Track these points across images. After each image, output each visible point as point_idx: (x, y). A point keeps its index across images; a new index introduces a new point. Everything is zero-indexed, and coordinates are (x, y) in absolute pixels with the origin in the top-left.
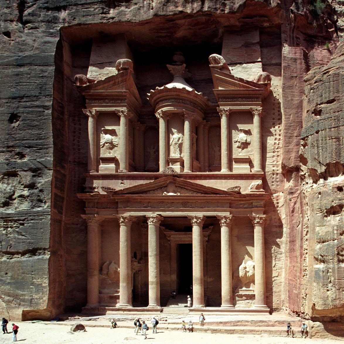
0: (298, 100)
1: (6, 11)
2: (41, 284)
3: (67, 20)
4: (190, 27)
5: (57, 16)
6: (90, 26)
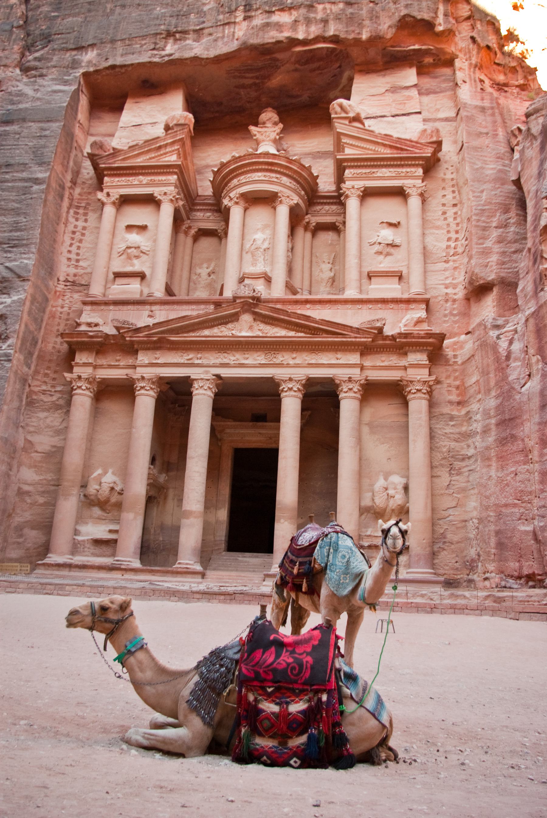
0: (495, 168)
3: (94, 62)
4: (297, 66)
5: (79, 59)
6: (130, 68)
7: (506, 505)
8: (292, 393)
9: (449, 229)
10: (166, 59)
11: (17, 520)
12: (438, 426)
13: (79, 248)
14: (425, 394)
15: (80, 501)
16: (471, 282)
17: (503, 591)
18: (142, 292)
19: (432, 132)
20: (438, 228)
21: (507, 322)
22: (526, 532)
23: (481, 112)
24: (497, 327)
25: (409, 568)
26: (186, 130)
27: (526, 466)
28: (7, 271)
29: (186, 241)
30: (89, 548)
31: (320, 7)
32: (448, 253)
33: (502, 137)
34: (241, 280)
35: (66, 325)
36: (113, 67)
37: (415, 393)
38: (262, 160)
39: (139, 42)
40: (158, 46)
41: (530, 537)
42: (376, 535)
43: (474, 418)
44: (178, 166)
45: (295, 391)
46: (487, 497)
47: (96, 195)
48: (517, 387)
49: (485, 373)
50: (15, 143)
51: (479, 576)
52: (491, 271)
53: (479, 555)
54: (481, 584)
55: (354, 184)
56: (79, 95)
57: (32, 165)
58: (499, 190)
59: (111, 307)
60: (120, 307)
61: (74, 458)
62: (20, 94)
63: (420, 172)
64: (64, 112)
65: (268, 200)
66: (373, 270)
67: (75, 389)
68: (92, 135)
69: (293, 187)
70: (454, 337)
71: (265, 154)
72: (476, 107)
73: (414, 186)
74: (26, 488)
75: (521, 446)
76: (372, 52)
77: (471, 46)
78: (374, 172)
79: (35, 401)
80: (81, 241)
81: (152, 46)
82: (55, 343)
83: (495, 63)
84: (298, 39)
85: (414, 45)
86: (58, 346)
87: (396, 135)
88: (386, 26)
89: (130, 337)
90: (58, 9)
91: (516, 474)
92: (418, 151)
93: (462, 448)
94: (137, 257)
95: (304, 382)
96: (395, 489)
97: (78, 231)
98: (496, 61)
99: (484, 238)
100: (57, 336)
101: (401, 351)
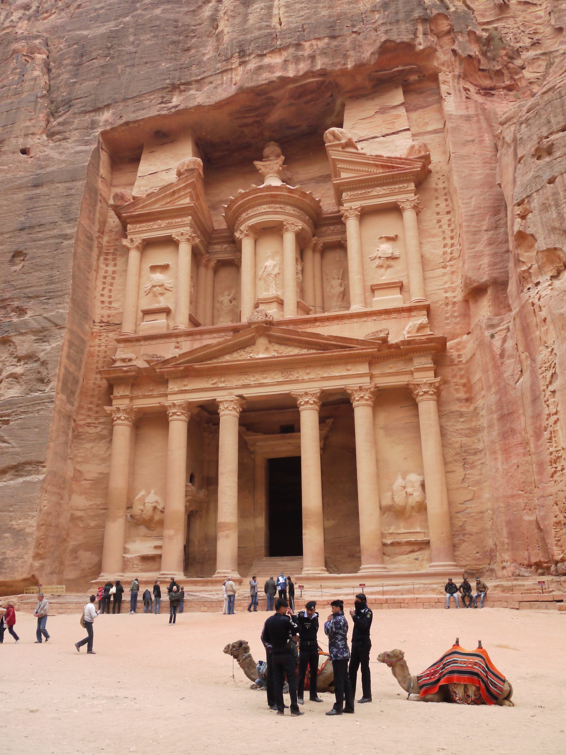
1: (28, 123)
2: (23, 529)
3: (110, 121)
4: (292, 101)
5: (97, 119)
6: (142, 123)
7: (513, 496)
8: (309, 406)
9: (444, 236)
10: (173, 110)
11: (72, 544)
12: (449, 424)
13: (110, 291)
14: (432, 395)
15: (127, 521)
16: (466, 285)
17: (517, 580)
18: (168, 326)
19: (420, 147)
20: (434, 236)
21: (502, 320)
22: (530, 522)
23: (467, 120)
24: (492, 326)
25: (431, 562)
26: (195, 174)
27: (525, 458)
28: (46, 321)
29: (206, 274)
30: (137, 565)
31: (307, 44)
32: (445, 259)
33: (488, 142)
35: (104, 362)
36: (127, 123)
37: (422, 395)
38: (266, 193)
39: (148, 98)
40: (165, 99)
41: (534, 526)
42: (398, 532)
43: (481, 414)
45: (311, 404)
46: (497, 489)
47: (121, 242)
48: (512, 382)
49: (485, 371)
50: (46, 204)
51: (498, 566)
52: (484, 273)
53: (496, 546)
54: (500, 573)
55: (352, 205)
56: (99, 152)
57: (62, 223)
58: (487, 194)
59: (142, 343)
60: (150, 342)
61: (118, 482)
62: (47, 158)
63: (412, 186)
64: (86, 171)
66: (375, 283)
67: (116, 420)
68: (115, 186)
69: (297, 214)
70: (457, 338)
72: (461, 117)
73: (408, 200)
74: (79, 514)
75: (520, 439)
76: (359, 79)
77: (453, 58)
78: (369, 192)
79: (81, 434)
80: (112, 284)
81: (160, 101)
82: (96, 379)
83: (480, 70)
85: (397, 67)
86: (99, 382)
87: (386, 154)
88: (368, 54)
89: (160, 368)
90: (76, 76)
91: (518, 466)
92: (409, 167)
93: (474, 443)
94: (162, 294)
95: (318, 395)
96: (413, 487)
97: (109, 276)
98: (481, 67)
99: (475, 242)
100: (97, 373)
101: (407, 357)
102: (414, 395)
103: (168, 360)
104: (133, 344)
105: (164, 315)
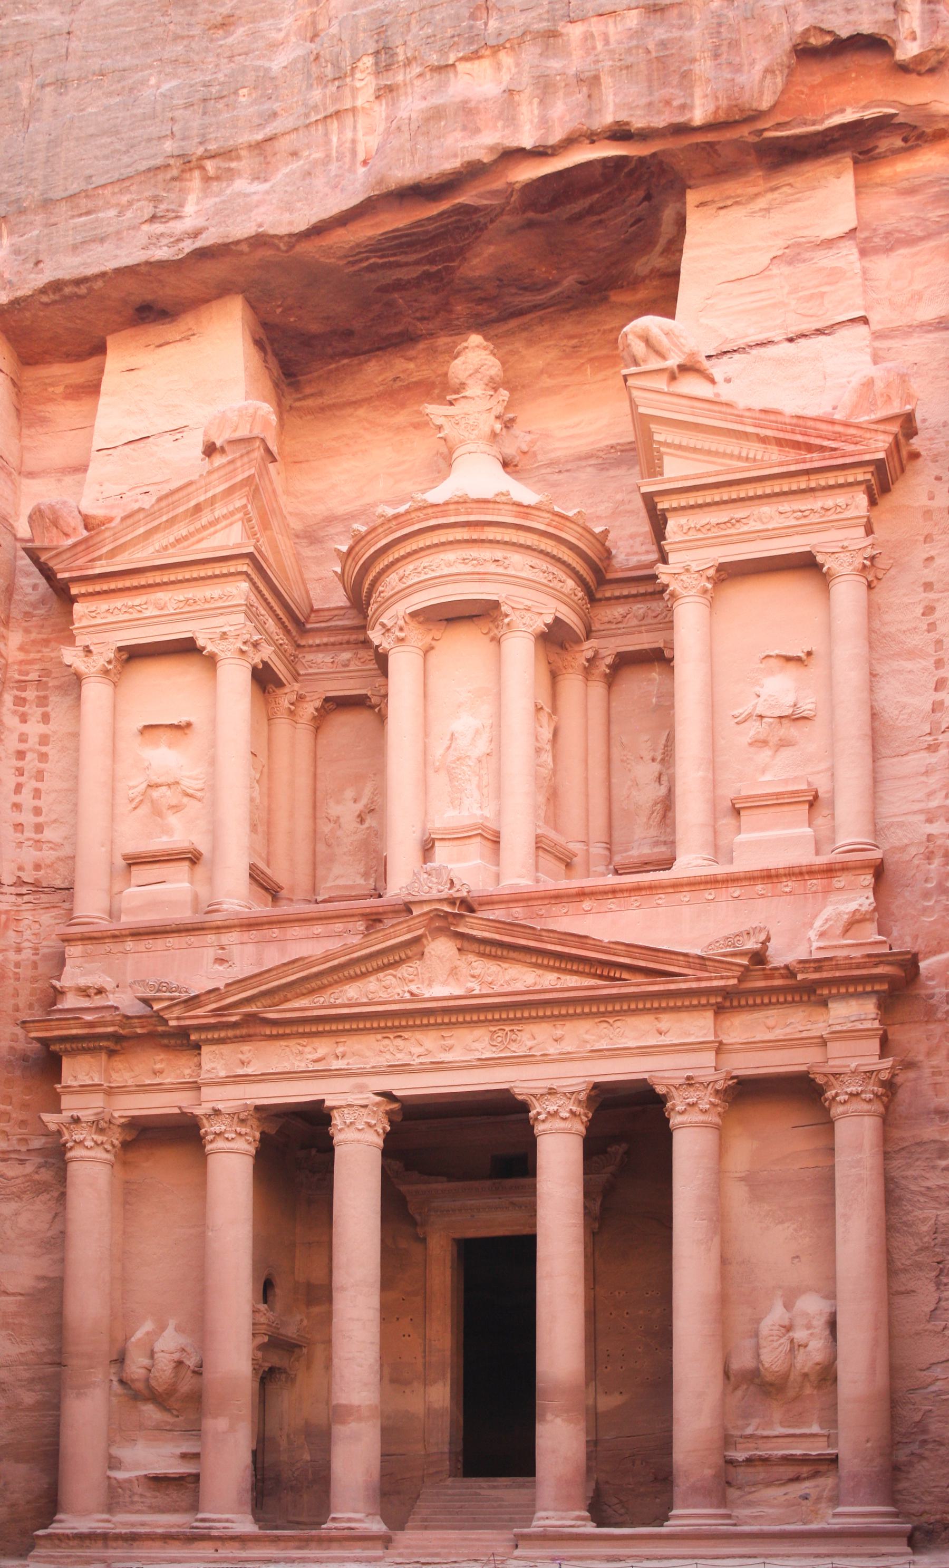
12: (910, 1173)
13: (37, 793)
34: (427, 849)
44: (250, 556)
60: (150, 943)
65: (480, 614)
71: (457, 503)
84: (523, 150)
89: (178, 1018)
94: (176, 808)
102: (826, 1100)
103: (197, 997)
104: (107, 947)
105: (186, 865)
